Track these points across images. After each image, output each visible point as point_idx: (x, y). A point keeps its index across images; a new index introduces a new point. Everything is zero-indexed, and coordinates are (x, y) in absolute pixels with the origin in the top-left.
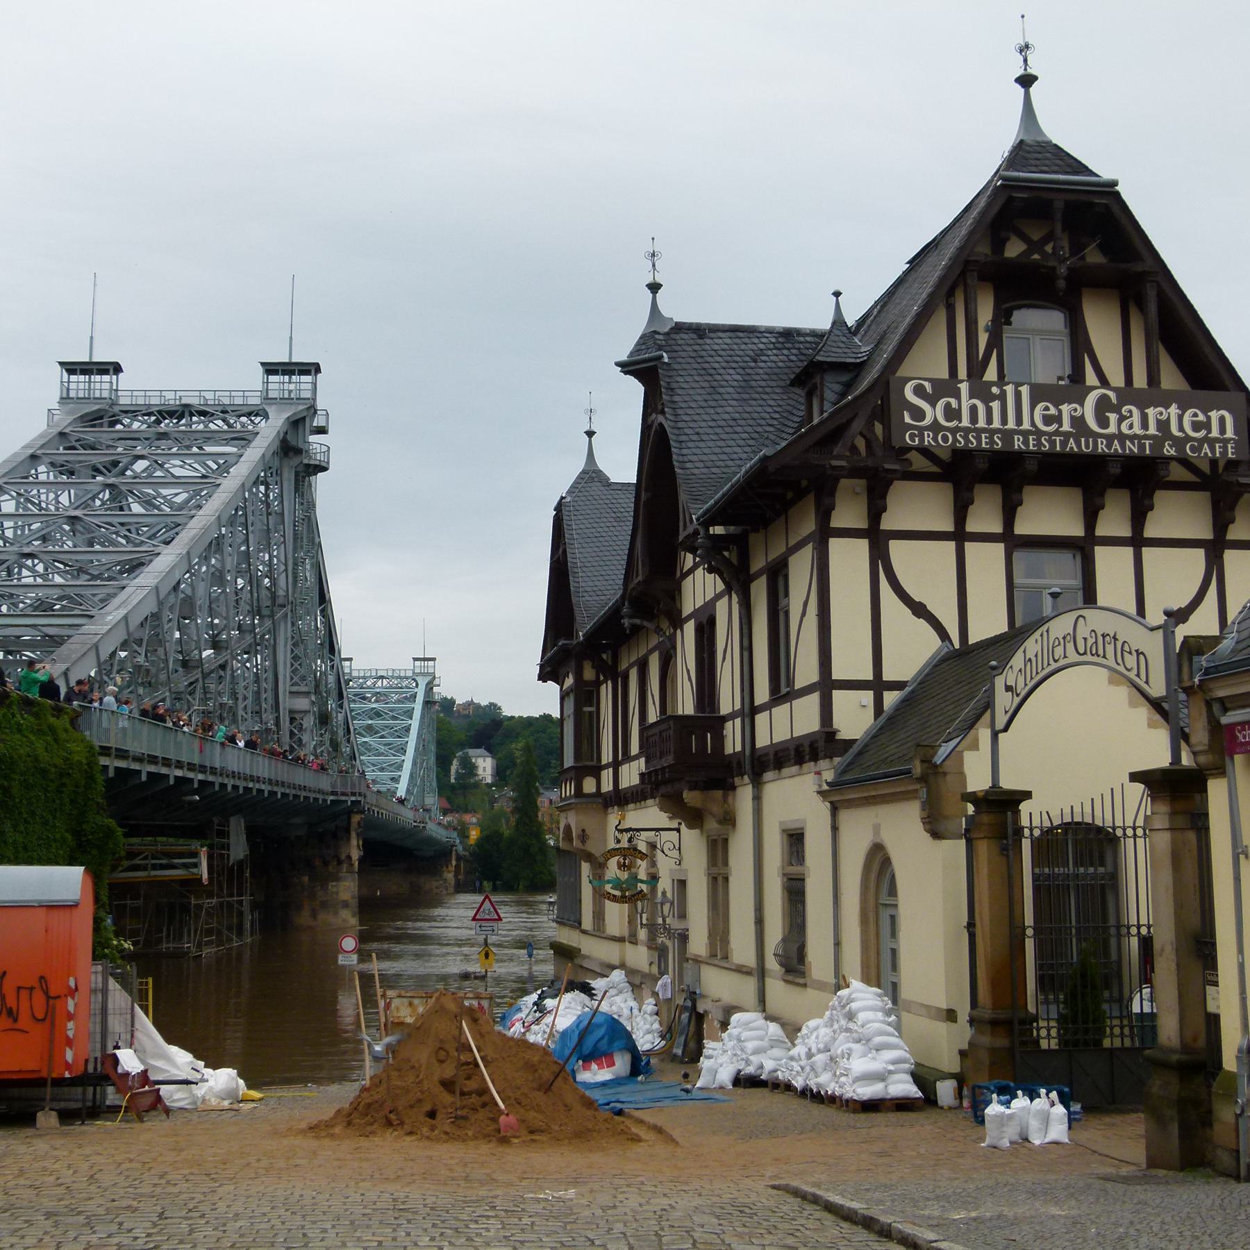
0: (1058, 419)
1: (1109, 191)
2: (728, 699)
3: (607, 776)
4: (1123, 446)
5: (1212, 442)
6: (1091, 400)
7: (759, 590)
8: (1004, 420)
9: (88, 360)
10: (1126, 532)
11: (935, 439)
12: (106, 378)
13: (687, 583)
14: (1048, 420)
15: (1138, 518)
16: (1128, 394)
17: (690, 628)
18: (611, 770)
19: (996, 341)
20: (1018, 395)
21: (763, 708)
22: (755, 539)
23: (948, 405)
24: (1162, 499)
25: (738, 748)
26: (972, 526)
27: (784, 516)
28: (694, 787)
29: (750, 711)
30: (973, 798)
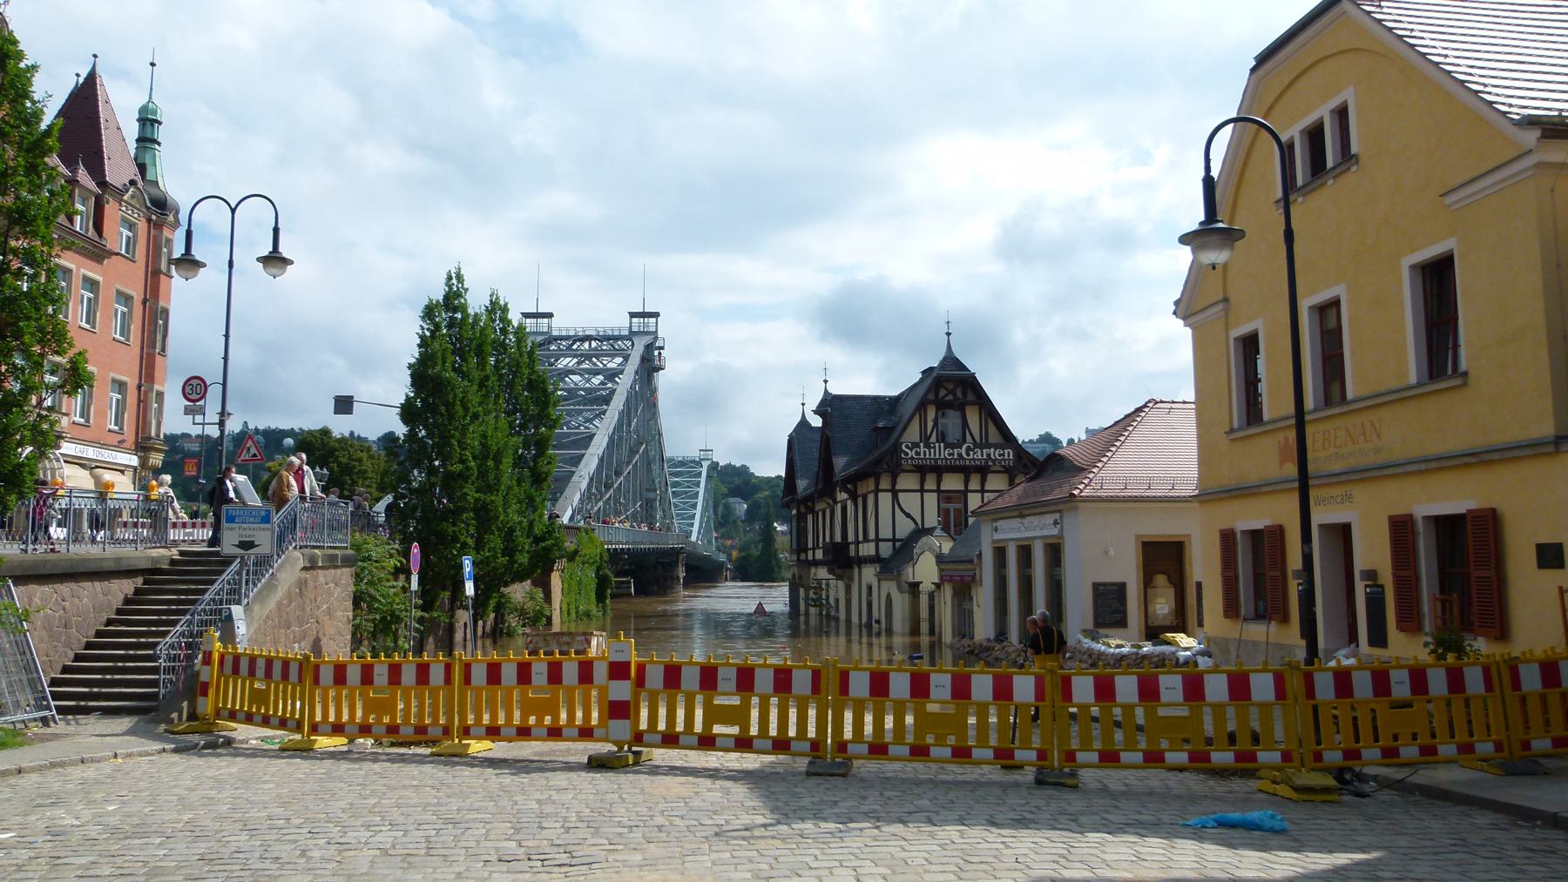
0: (953, 454)
1: (973, 376)
2: (851, 538)
3: (810, 553)
4: (974, 462)
5: (1005, 460)
7: (860, 501)
9: (535, 311)
10: (979, 488)
12: (546, 320)
14: (949, 455)
15: (983, 484)
16: (976, 445)
17: (839, 505)
19: (936, 424)
20: (940, 447)
21: (861, 542)
22: (859, 483)
24: (990, 477)
26: (926, 487)
28: (839, 568)
29: (857, 543)
30: (906, 582)
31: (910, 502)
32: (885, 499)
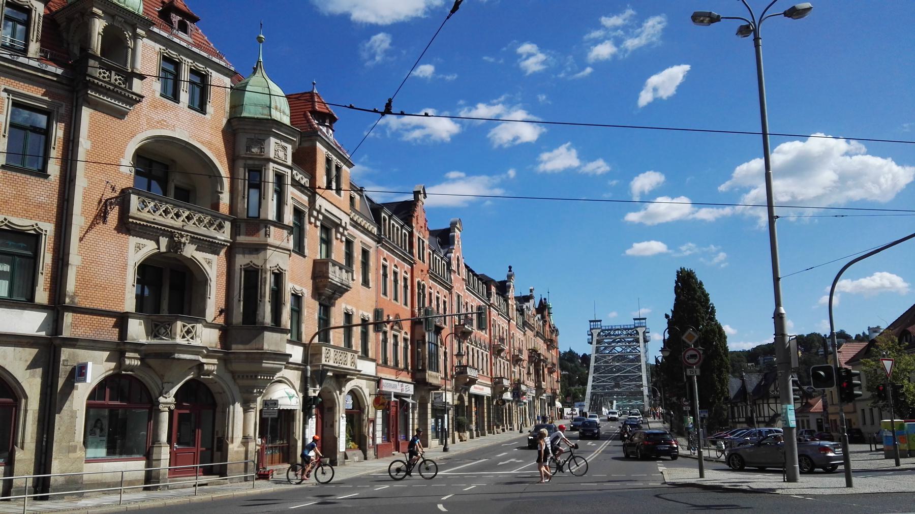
31: (773, 406)
32: (766, 406)
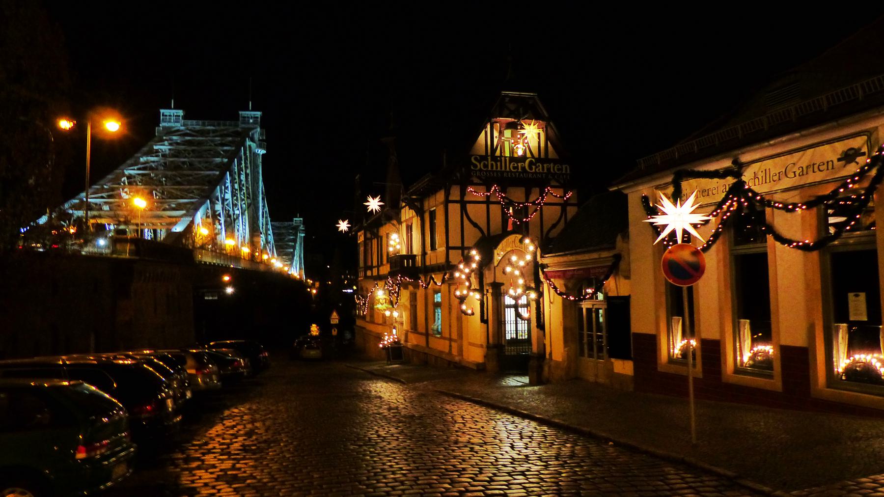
3: (375, 271)
6: (527, 161)
7: (427, 217)
8: (501, 168)
11: (480, 174)
13: (403, 211)
18: (376, 268)
23: (485, 163)
25: (420, 265)
27: (434, 196)
